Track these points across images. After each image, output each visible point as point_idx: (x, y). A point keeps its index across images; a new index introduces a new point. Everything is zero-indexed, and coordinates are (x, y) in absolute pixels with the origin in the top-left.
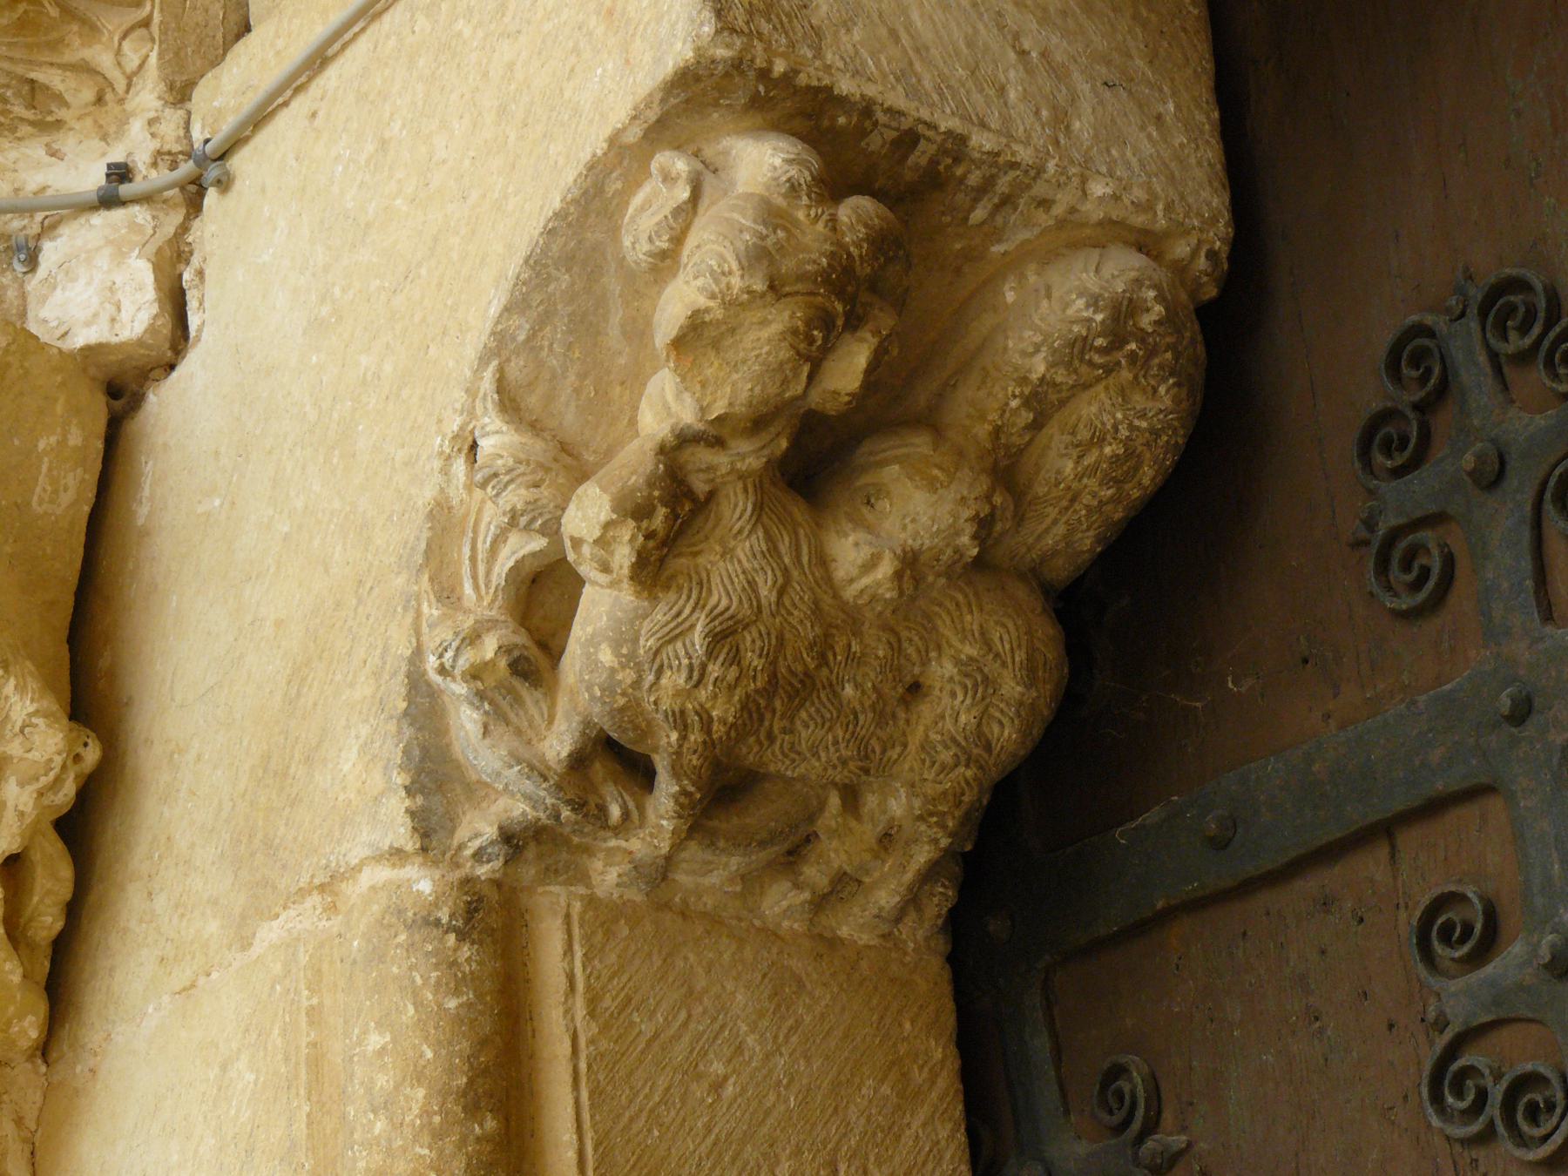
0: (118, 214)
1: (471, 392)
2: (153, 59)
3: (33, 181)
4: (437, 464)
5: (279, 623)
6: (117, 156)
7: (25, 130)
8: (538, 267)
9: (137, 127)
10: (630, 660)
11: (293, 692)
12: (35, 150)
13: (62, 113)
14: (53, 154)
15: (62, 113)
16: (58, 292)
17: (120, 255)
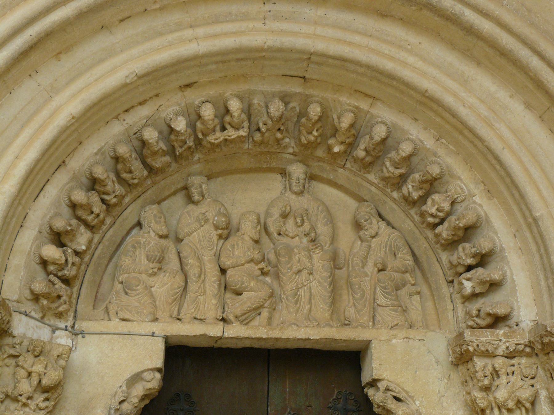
0: (66, 332)
1: (123, 382)
2: (72, 314)
3: (57, 323)
4: (117, 387)
5: (88, 392)
6: (67, 325)
7: (58, 317)
8: (135, 375)
9: (69, 322)
10: (130, 412)
11: (90, 400)
12: (58, 320)
13: (62, 317)
14: (60, 321)
15: (62, 317)
16: (59, 339)
17: (67, 338)
